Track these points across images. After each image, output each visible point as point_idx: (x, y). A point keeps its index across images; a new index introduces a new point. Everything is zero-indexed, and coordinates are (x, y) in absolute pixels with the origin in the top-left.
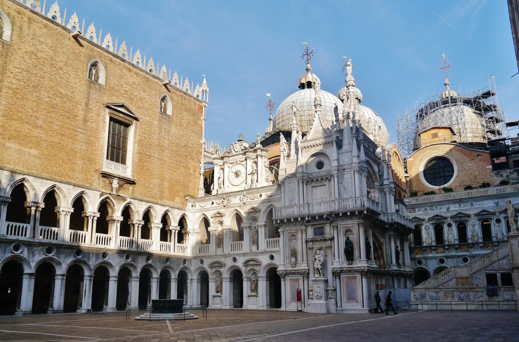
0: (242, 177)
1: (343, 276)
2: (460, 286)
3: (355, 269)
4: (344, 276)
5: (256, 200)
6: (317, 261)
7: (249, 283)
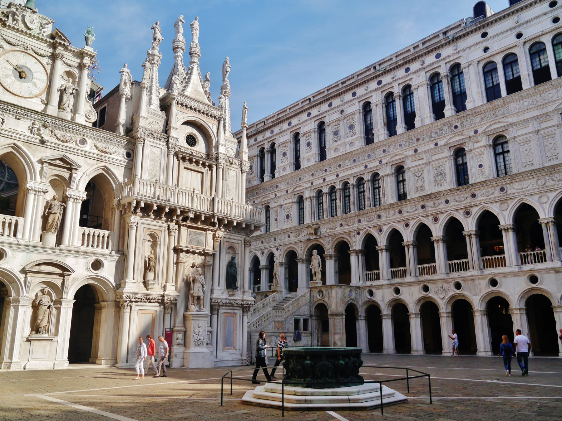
0: (35, 85)
1: (221, 311)
2: (276, 330)
3: (240, 303)
4: (223, 311)
5: (69, 144)
6: (198, 285)
7: (30, 311)
